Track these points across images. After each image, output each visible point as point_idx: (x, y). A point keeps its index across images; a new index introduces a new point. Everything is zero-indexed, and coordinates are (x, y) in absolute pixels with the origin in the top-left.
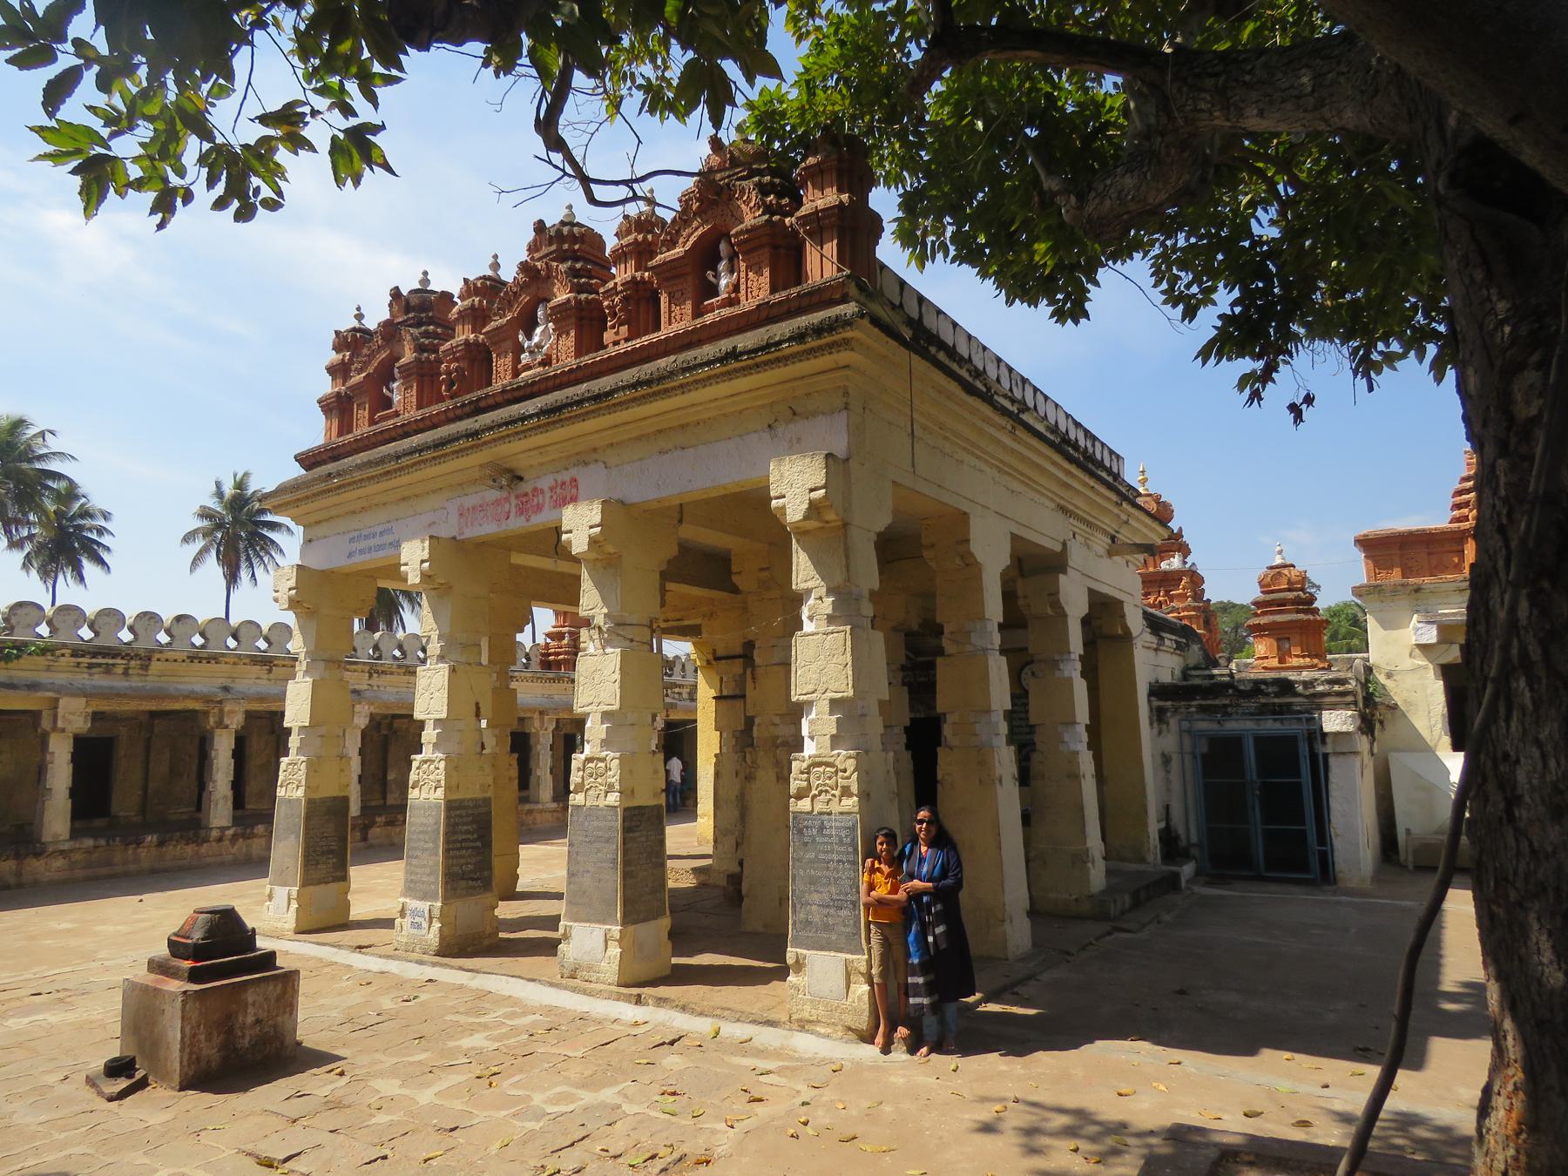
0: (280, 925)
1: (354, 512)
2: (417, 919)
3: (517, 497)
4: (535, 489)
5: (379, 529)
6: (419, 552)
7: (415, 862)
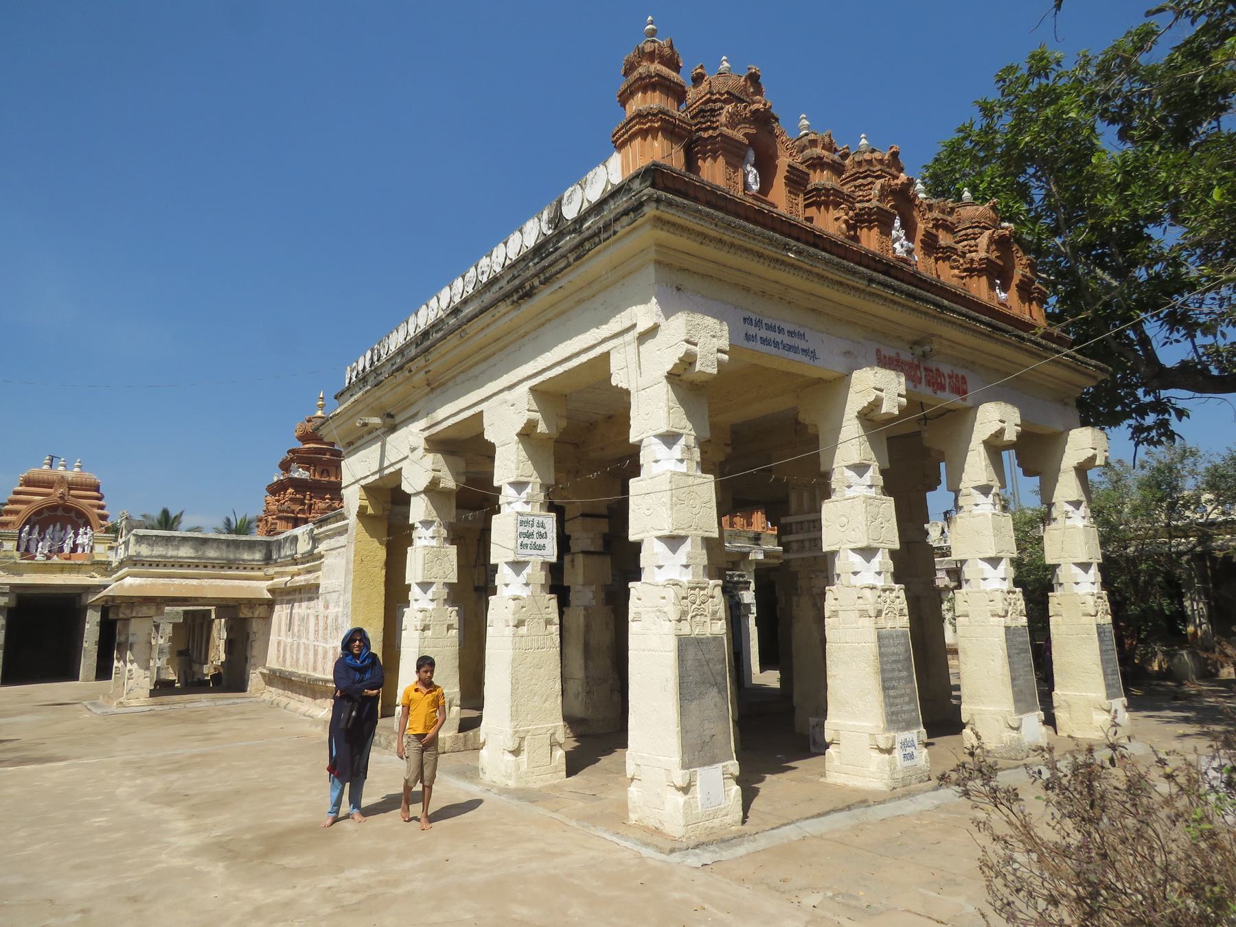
0: (716, 822)
1: (747, 289)
2: (909, 750)
3: (926, 369)
4: (938, 370)
5: (787, 327)
6: (895, 384)
7: (892, 693)
